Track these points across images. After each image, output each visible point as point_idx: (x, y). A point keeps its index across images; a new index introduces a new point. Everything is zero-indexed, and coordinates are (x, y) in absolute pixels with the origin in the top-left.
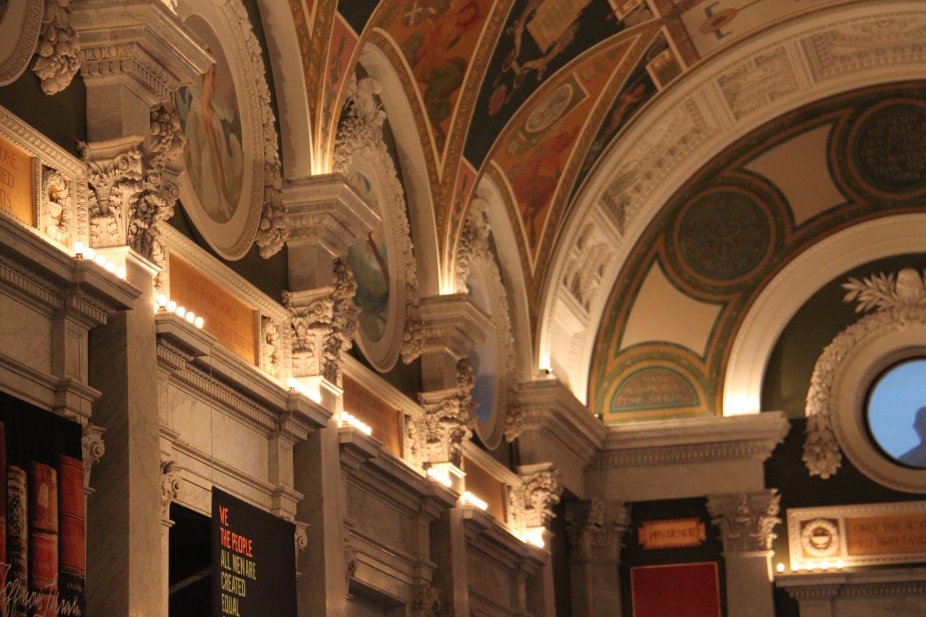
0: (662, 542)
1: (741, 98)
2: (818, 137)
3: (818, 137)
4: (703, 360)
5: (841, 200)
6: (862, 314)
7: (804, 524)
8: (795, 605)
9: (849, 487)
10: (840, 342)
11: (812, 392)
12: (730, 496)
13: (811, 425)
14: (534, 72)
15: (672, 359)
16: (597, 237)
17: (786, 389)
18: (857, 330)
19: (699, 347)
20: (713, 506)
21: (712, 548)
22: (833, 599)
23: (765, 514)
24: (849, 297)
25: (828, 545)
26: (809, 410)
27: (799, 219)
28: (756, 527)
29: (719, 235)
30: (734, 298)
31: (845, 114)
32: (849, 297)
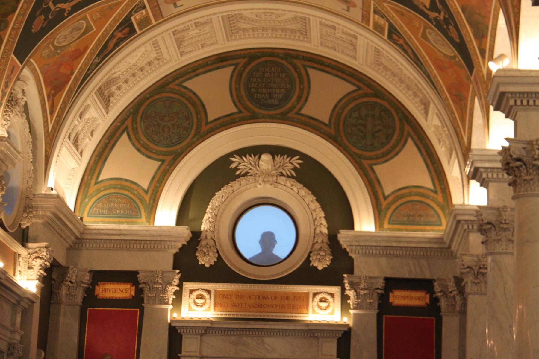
0: (108, 295)
1: (185, 44)
2: (226, 72)
3: (226, 72)
4: (146, 192)
5: (235, 110)
6: (239, 176)
7: (191, 292)
8: (180, 336)
9: (220, 272)
10: (225, 190)
11: (206, 217)
12: (152, 272)
13: (203, 236)
14: (63, 10)
16: (92, 113)
17: (192, 213)
18: (235, 185)
19: (145, 185)
20: (141, 277)
21: (138, 301)
23: (170, 284)
24: (233, 166)
25: (203, 305)
26: (204, 227)
27: (211, 118)
28: (164, 291)
29: (163, 120)
30: (169, 158)
31: (242, 61)
32: (233, 166)
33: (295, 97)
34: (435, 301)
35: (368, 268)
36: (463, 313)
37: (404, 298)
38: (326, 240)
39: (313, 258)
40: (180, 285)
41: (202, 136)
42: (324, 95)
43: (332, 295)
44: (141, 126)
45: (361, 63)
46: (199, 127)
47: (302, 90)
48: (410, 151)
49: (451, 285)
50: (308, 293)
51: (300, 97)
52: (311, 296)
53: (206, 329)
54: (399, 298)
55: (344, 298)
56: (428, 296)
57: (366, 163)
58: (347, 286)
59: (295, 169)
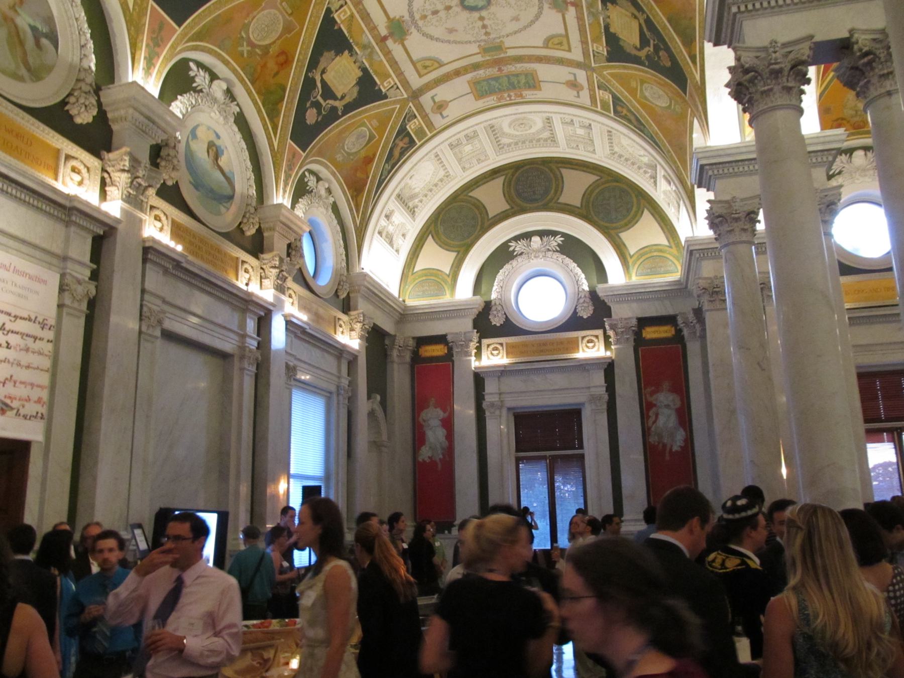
0: (428, 354)
1: (464, 160)
2: (499, 181)
3: (499, 181)
4: (448, 276)
6: (516, 256)
7: (488, 346)
8: (483, 379)
10: (507, 267)
11: (494, 288)
12: (457, 334)
13: (493, 303)
15: (436, 276)
17: (484, 288)
18: (514, 262)
19: (447, 270)
20: (449, 338)
21: (449, 357)
22: (499, 377)
23: (471, 341)
24: (511, 249)
25: (498, 354)
26: (494, 296)
27: (491, 216)
28: (467, 346)
29: (457, 221)
30: (463, 249)
31: (511, 171)
32: (511, 249)
33: (553, 192)
34: (679, 331)
35: (624, 313)
36: (703, 337)
37: (654, 332)
38: (588, 295)
39: (579, 309)
40: (480, 342)
41: (484, 230)
42: (575, 187)
43: (597, 337)
44: (441, 229)
45: (600, 156)
46: (483, 223)
47: (557, 186)
48: (647, 218)
49: (691, 317)
50: (578, 338)
51: (556, 191)
52: (580, 339)
53: (502, 372)
54: (650, 333)
55: (606, 338)
56: (673, 329)
57: (612, 232)
58: (607, 327)
59: (559, 245)
